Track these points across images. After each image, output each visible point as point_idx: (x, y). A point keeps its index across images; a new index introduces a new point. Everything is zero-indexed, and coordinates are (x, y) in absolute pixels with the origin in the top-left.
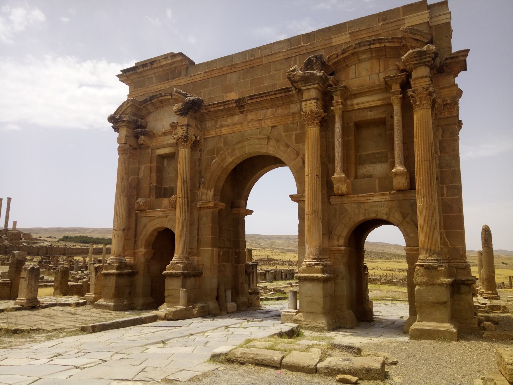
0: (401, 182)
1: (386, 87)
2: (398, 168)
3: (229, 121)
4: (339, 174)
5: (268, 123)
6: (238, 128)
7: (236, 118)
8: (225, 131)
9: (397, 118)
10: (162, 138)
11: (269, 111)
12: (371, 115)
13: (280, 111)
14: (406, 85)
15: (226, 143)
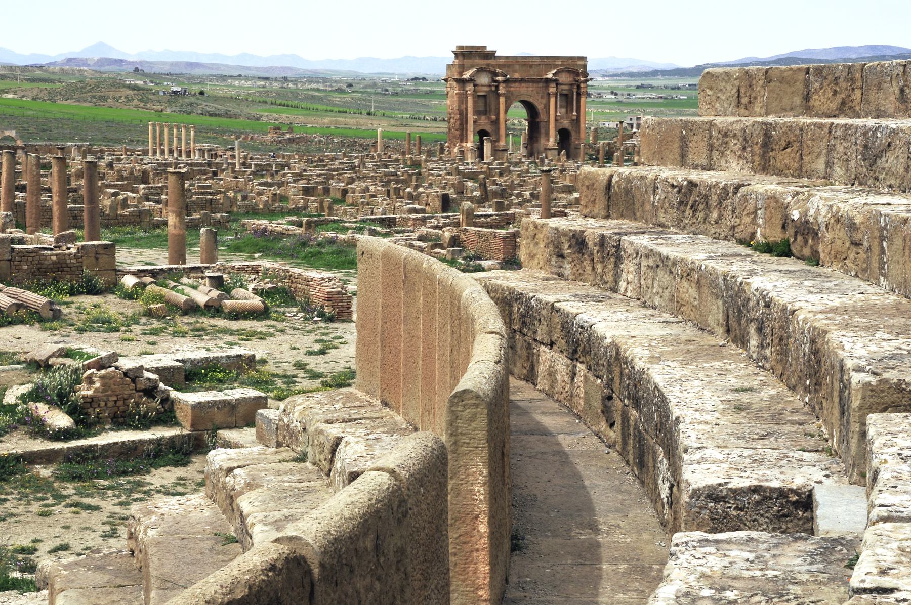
0: (575, 118)
1: (572, 85)
2: (575, 113)
3: (513, 85)
4: (558, 114)
5: (531, 89)
6: (518, 89)
7: (517, 84)
8: (512, 89)
9: (575, 97)
10: (480, 87)
11: (531, 84)
12: (565, 92)
13: (535, 85)
14: (579, 86)
15: (512, 94)
